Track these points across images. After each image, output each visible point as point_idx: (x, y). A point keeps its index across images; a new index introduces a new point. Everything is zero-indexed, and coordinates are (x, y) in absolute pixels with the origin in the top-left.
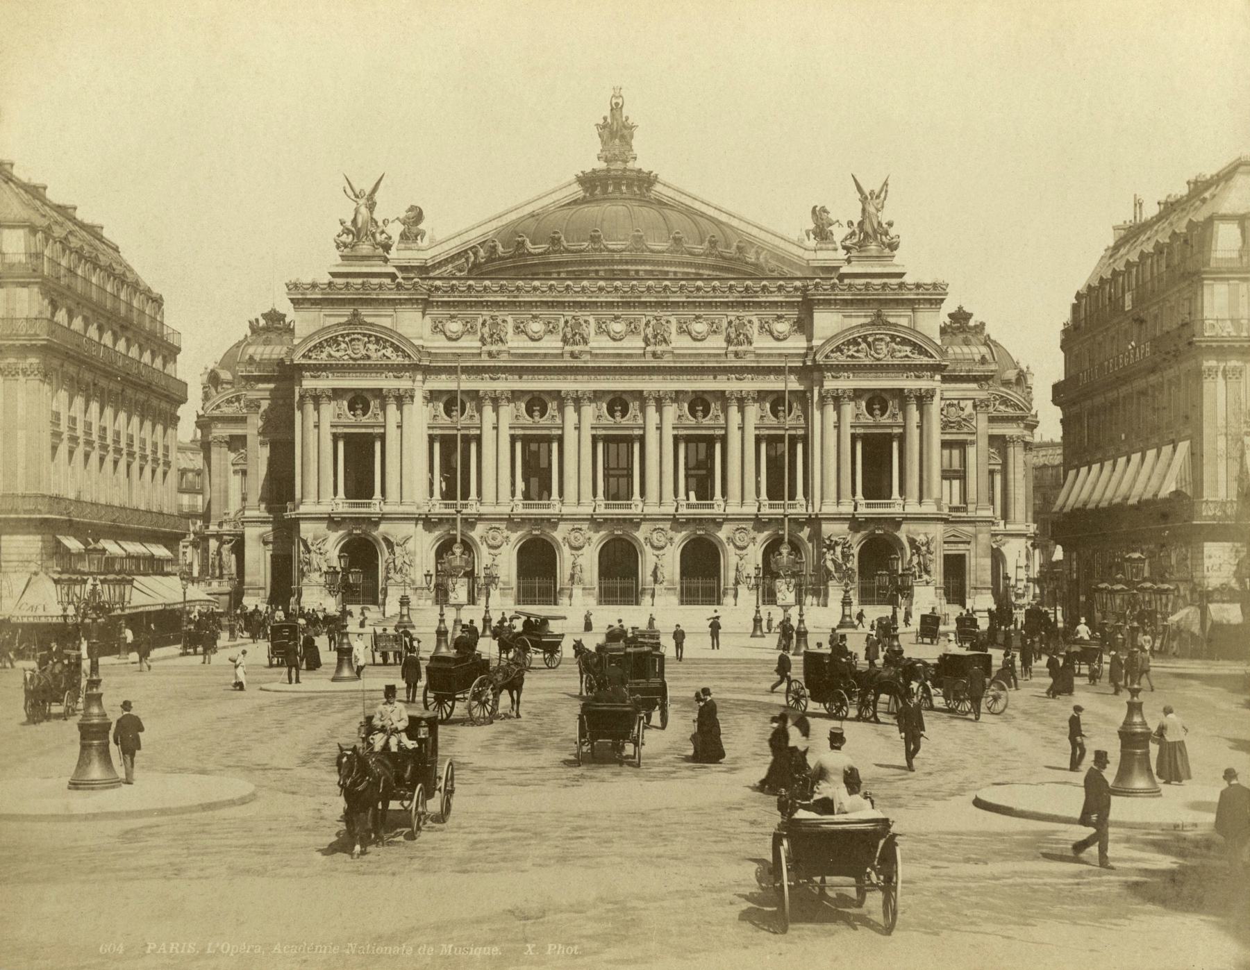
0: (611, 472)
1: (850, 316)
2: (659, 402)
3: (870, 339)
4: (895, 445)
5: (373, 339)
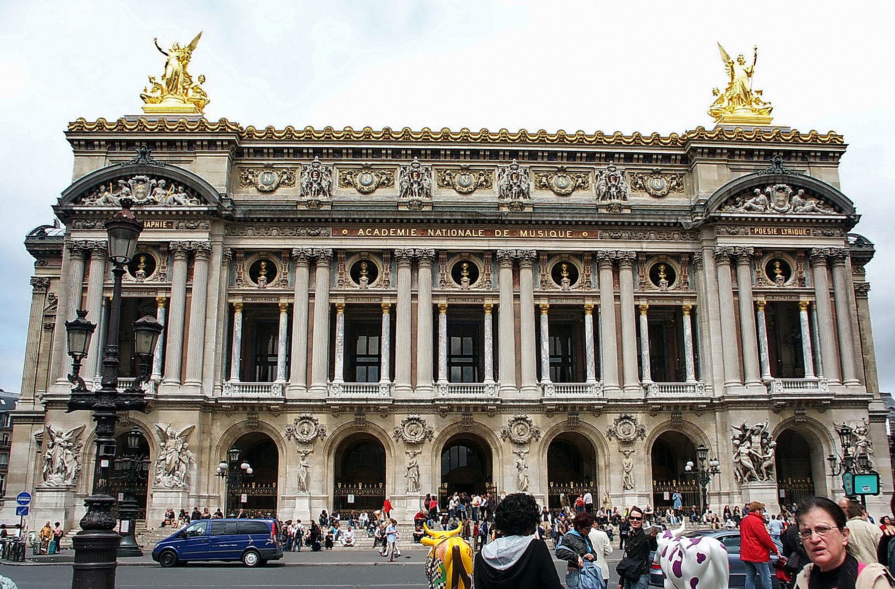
0: (454, 360)
1: (740, 170)
2: (516, 265)
3: (768, 189)
4: (804, 315)
5: (162, 181)
